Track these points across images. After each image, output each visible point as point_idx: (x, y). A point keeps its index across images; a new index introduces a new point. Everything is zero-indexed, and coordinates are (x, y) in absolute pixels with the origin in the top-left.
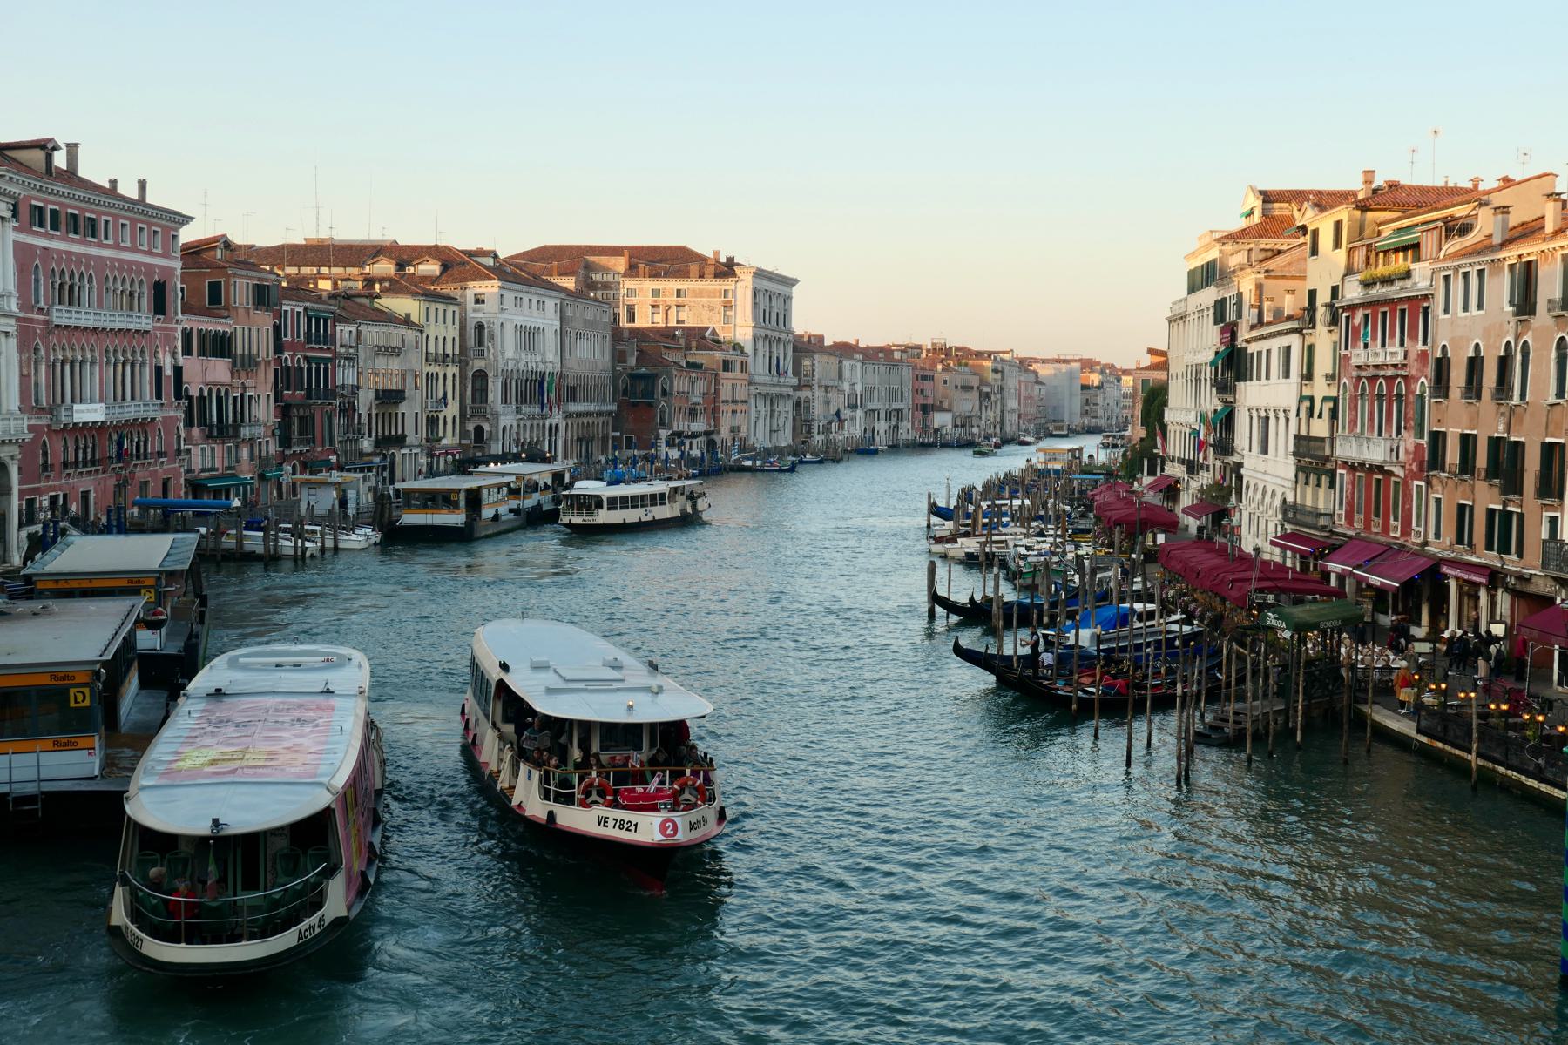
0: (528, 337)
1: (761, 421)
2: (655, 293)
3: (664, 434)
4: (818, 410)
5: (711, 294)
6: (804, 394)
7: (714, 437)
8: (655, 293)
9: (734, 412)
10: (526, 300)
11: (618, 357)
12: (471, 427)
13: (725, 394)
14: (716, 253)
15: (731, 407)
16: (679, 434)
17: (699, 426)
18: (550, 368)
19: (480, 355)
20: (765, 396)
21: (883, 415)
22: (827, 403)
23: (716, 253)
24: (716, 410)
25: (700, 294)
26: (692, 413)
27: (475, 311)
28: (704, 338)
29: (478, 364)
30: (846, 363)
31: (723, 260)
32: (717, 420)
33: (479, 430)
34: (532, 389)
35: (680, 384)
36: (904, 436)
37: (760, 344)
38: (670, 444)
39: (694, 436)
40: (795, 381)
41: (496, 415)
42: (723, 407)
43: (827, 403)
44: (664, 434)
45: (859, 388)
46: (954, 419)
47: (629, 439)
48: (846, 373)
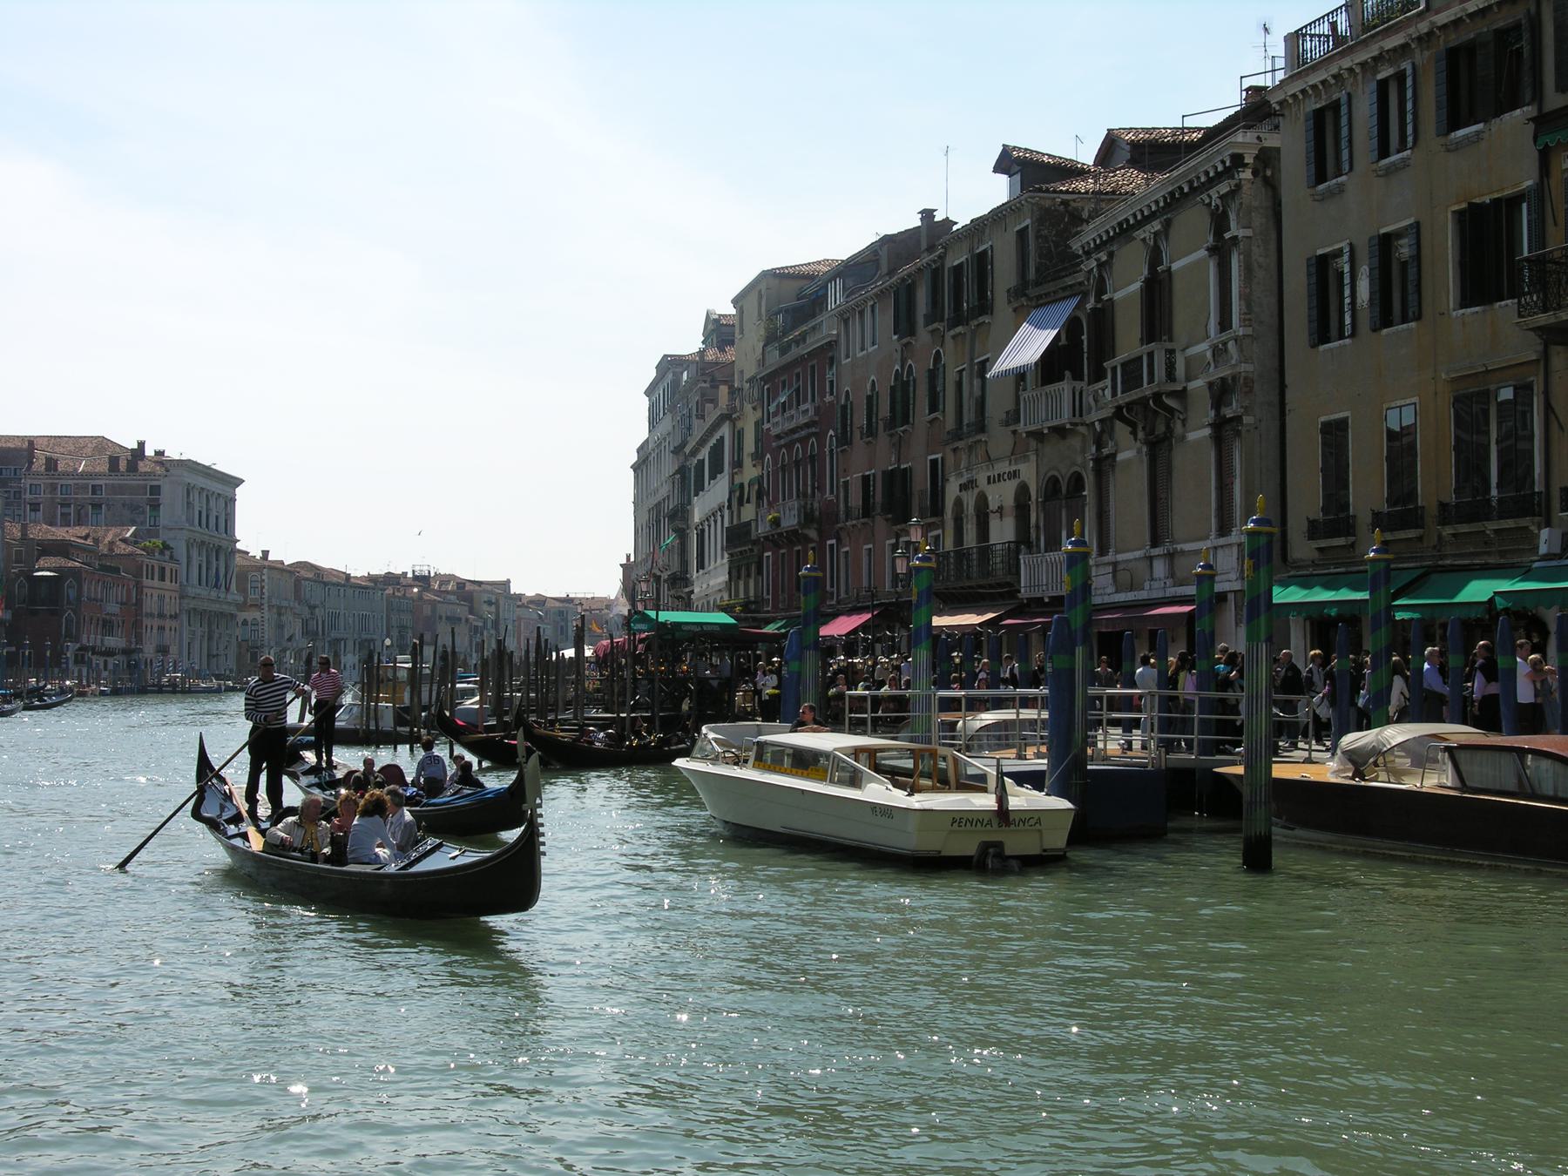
1: (197, 645)
3: (72, 647)
6: (250, 615)
9: (161, 628)
13: (150, 605)
15: (156, 622)
16: (94, 650)
20: (202, 613)
21: (350, 644)
22: (280, 627)
23: (141, 445)
24: (137, 624)
26: (107, 626)
32: (139, 639)
35: (91, 589)
37: (194, 553)
39: (110, 653)
42: (147, 622)
43: (280, 627)
44: (72, 647)
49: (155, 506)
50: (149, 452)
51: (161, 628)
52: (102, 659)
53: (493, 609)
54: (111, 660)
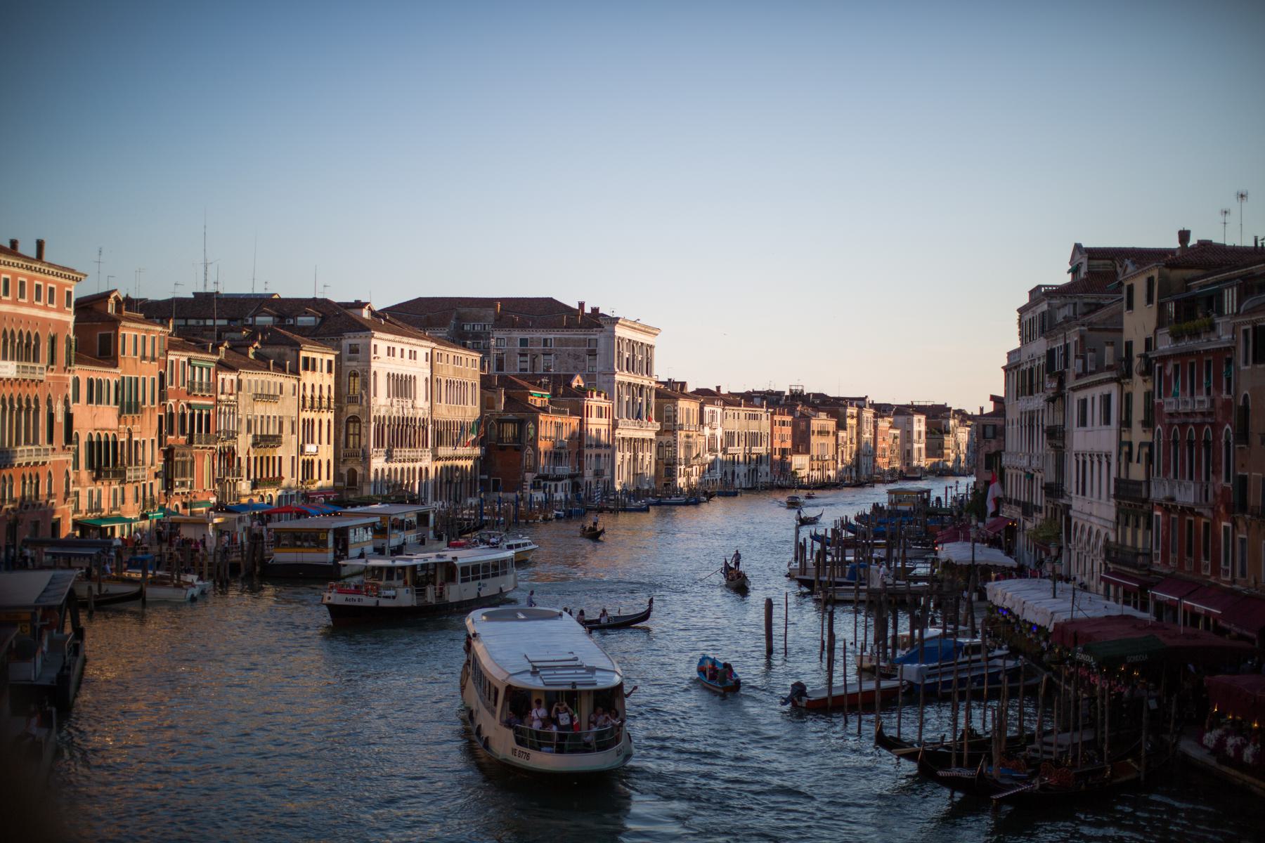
0: (401, 386)
2: (524, 342)
3: (529, 477)
4: (681, 453)
5: (577, 343)
6: (666, 438)
7: (578, 479)
8: (524, 342)
9: (598, 456)
10: (398, 352)
11: (486, 404)
12: (344, 470)
14: (582, 305)
15: (594, 451)
16: (546, 478)
17: (565, 469)
18: (420, 414)
19: (353, 400)
23: (582, 305)
24: (580, 454)
25: (566, 342)
27: (349, 360)
28: (570, 385)
29: (353, 410)
30: (707, 409)
31: (588, 310)
32: (581, 464)
33: (353, 473)
34: (401, 433)
36: (763, 479)
38: (536, 486)
39: (559, 479)
40: (657, 426)
41: (366, 459)
42: (587, 451)
44: (529, 477)
45: (719, 433)
46: (812, 459)
47: (496, 482)
48: (707, 419)
49: (593, 353)
50: (588, 310)
51: (598, 456)
52: (553, 484)
53: (854, 422)
54: (560, 484)
